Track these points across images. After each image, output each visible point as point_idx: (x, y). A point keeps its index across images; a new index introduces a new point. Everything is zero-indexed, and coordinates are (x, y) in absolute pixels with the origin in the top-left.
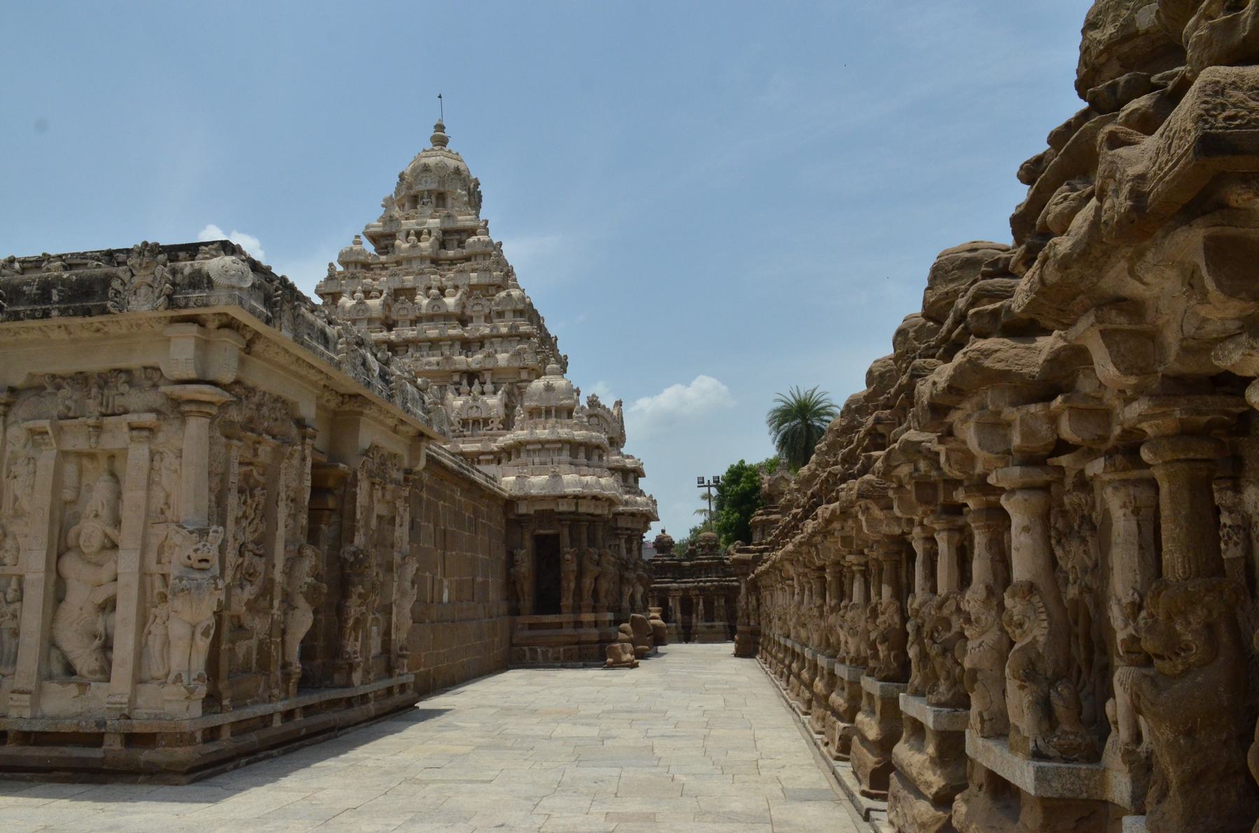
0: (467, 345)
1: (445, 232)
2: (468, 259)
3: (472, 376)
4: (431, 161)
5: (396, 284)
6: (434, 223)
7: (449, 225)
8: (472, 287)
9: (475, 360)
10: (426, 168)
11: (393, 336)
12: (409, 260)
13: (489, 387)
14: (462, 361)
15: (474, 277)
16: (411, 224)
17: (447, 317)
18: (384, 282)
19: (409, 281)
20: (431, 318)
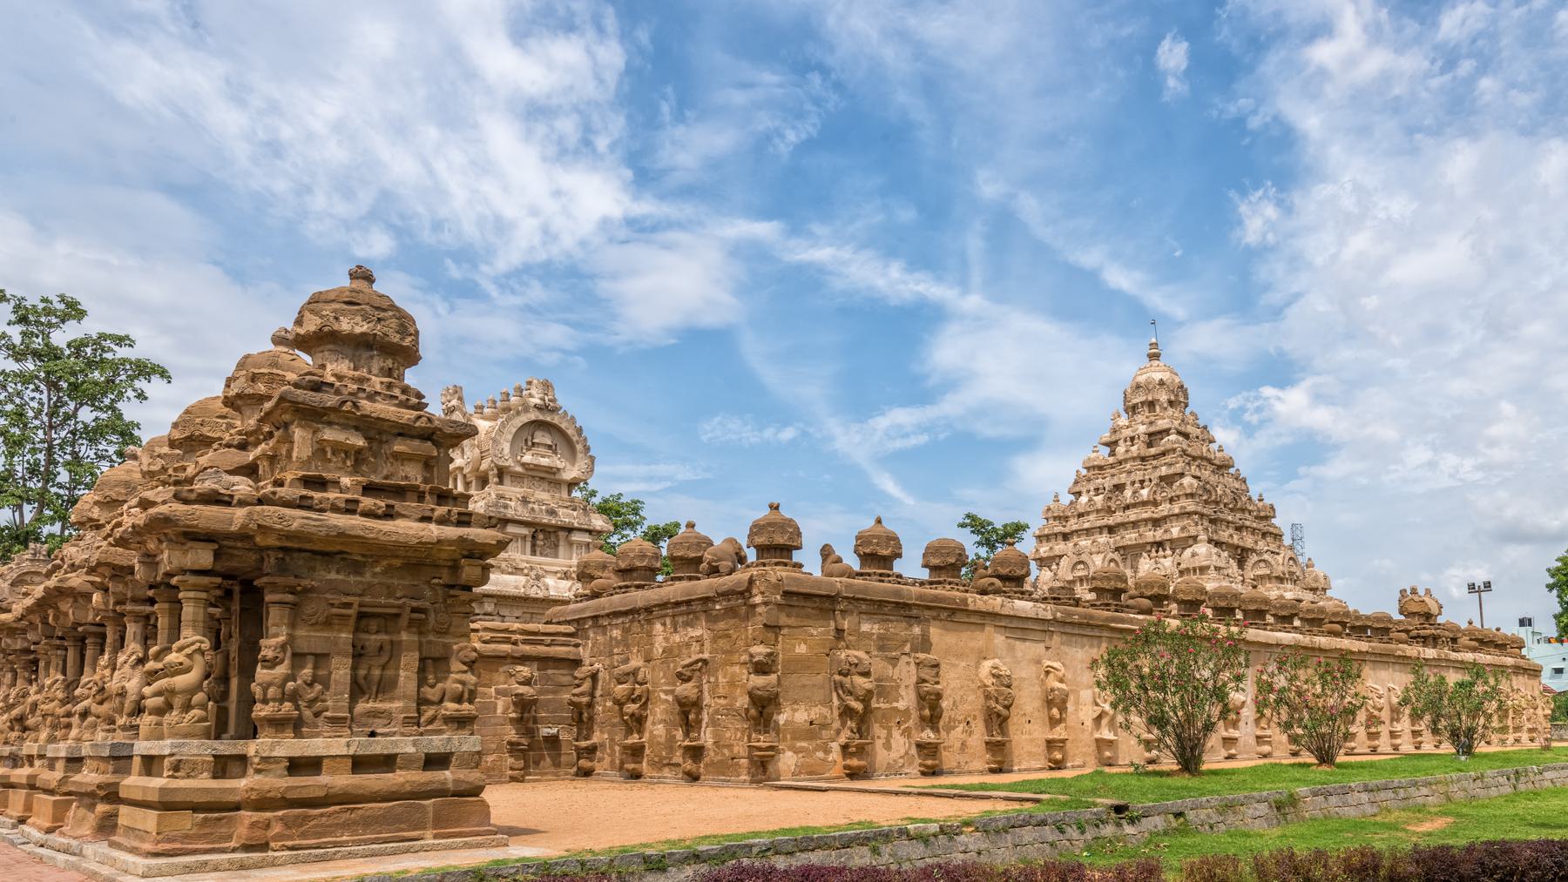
0: (1156, 522)
1: (1150, 435)
2: (1163, 454)
3: (1159, 545)
4: (1141, 379)
5: (1116, 481)
6: (1142, 429)
7: (1153, 429)
8: (1162, 478)
9: (1159, 534)
10: (1138, 387)
11: (1111, 521)
12: (1126, 461)
13: (1169, 552)
14: (1151, 535)
15: (1164, 471)
16: (1128, 433)
17: (1144, 504)
18: (1108, 483)
19: (1123, 478)
20: (1135, 505)
